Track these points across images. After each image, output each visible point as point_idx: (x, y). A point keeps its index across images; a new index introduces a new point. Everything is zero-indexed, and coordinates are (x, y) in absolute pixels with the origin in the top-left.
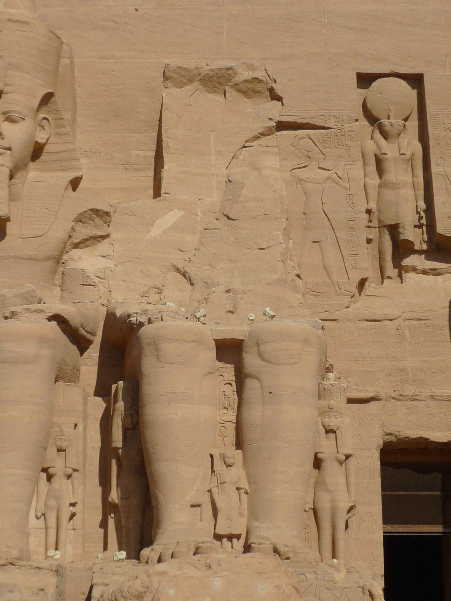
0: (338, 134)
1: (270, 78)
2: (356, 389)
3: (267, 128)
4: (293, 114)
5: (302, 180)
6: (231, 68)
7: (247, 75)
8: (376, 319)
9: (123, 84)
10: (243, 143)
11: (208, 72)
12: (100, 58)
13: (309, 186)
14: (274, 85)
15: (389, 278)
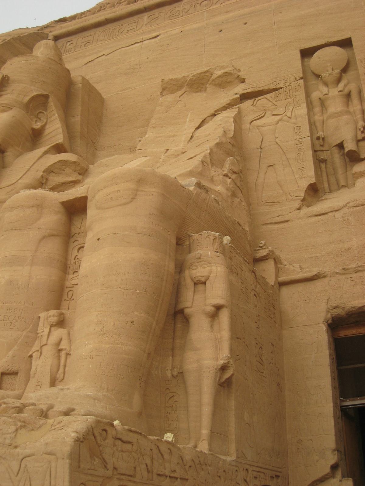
0: (287, 90)
1: (236, 70)
2: (301, 271)
3: (232, 99)
4: (254, 86)
5: (259, 126)
6: (207, 71)
7: (219, 73)
8: (323, 212)
9: (134, 101)
10: (212, 111)
11: (192, 78)
12: (121, 91)
13: (264, 129)
14: (239, 74)
15: (343, 186)
